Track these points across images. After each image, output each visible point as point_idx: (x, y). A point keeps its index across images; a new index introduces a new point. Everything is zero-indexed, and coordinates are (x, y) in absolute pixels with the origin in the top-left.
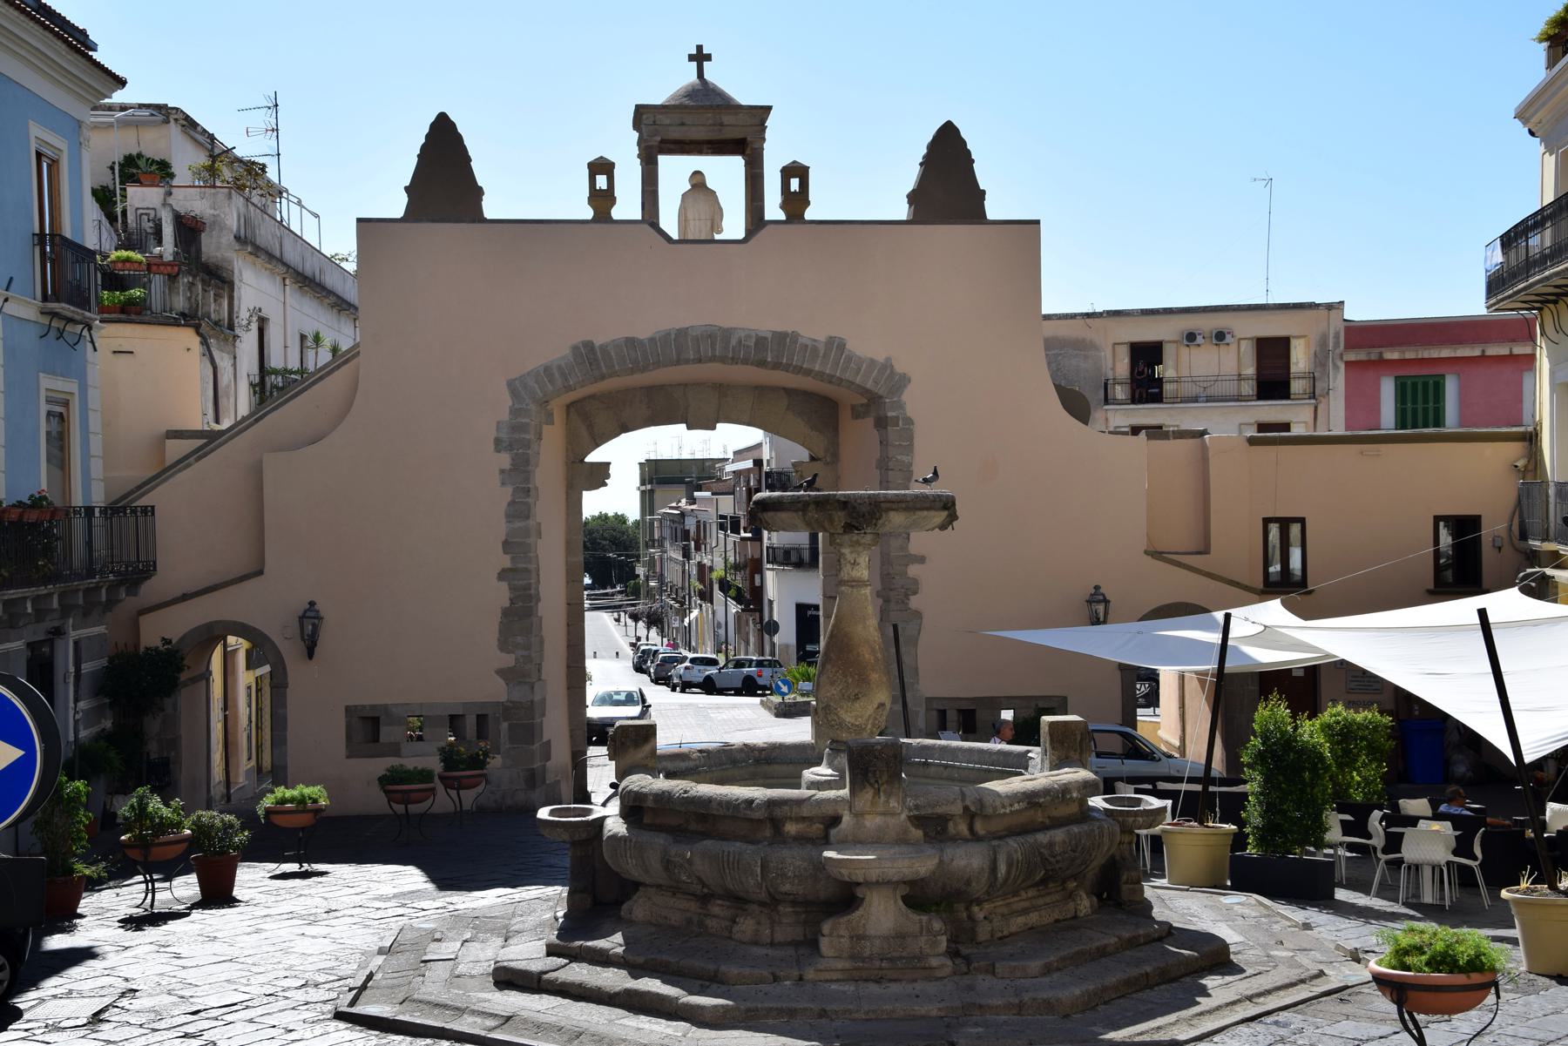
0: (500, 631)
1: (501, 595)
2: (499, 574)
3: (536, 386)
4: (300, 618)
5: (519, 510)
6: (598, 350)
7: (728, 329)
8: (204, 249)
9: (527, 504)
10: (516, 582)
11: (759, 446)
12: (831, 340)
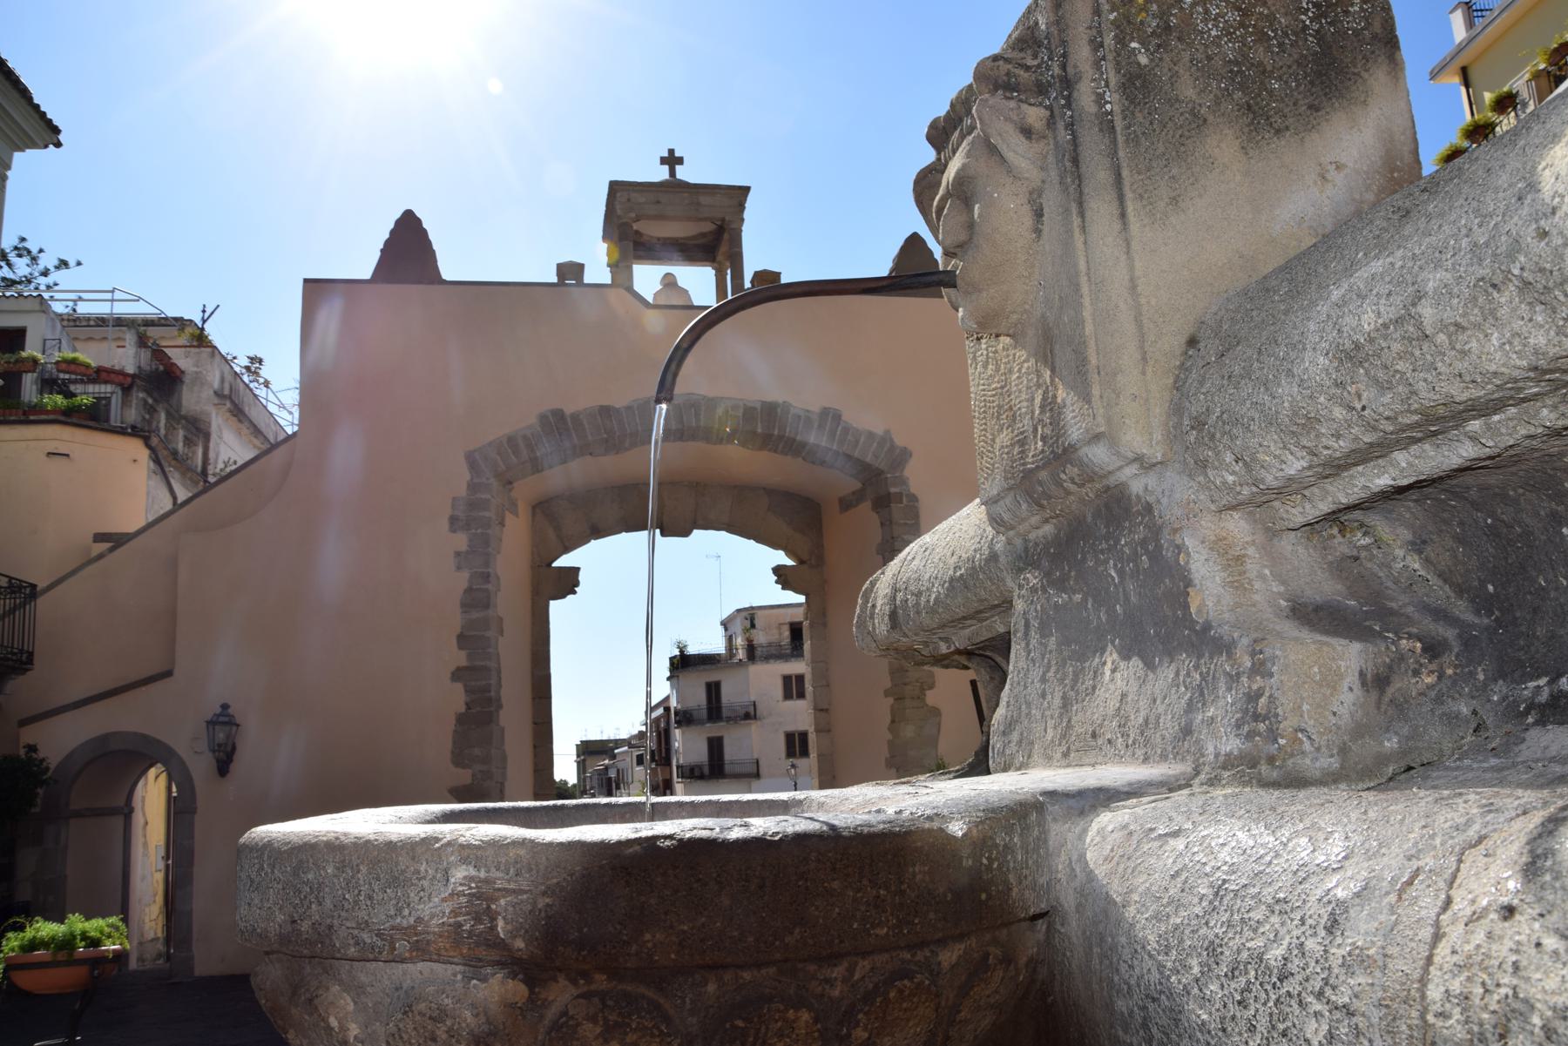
0: (454, 743)
1: (456, 699)
2: (453, 674)
3: (498, 458)
4: (208, 723)
5: (477, 599)
6: (569, 419)
7: (712, 399)
8: (184, 403)
9: (487, 590)
10: (473, 683)
11: (667, 699)
12: (825, 412)
